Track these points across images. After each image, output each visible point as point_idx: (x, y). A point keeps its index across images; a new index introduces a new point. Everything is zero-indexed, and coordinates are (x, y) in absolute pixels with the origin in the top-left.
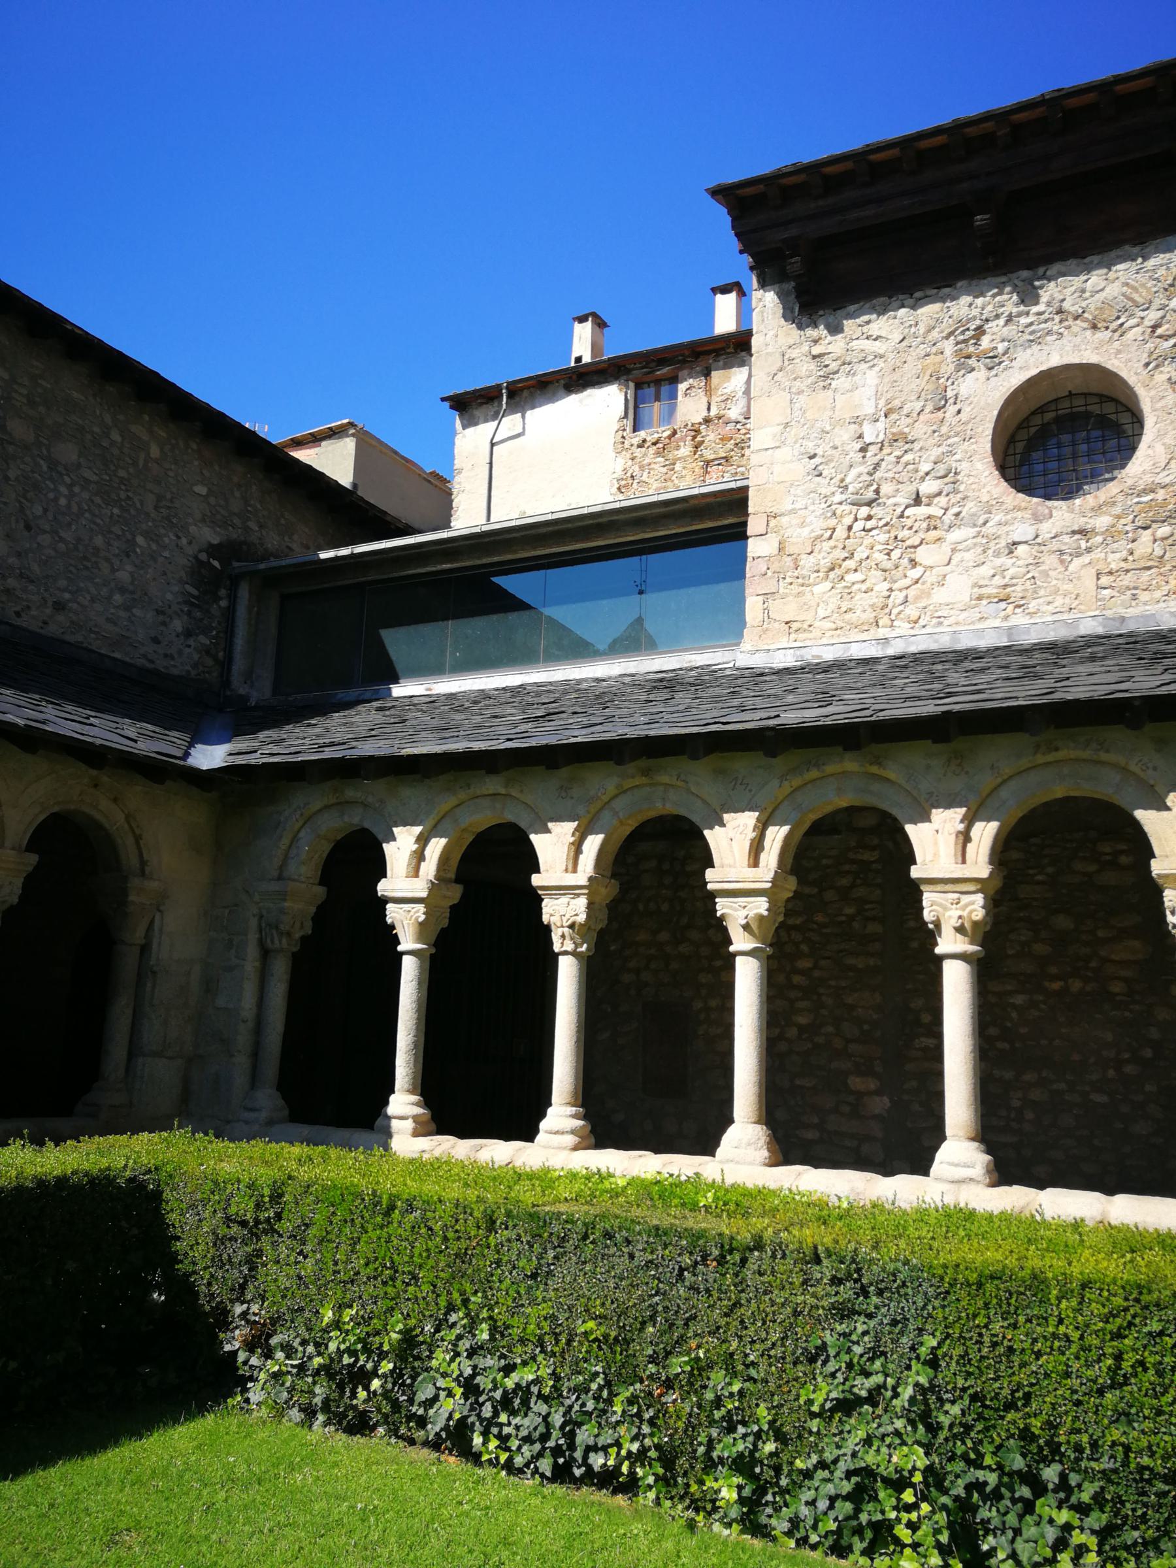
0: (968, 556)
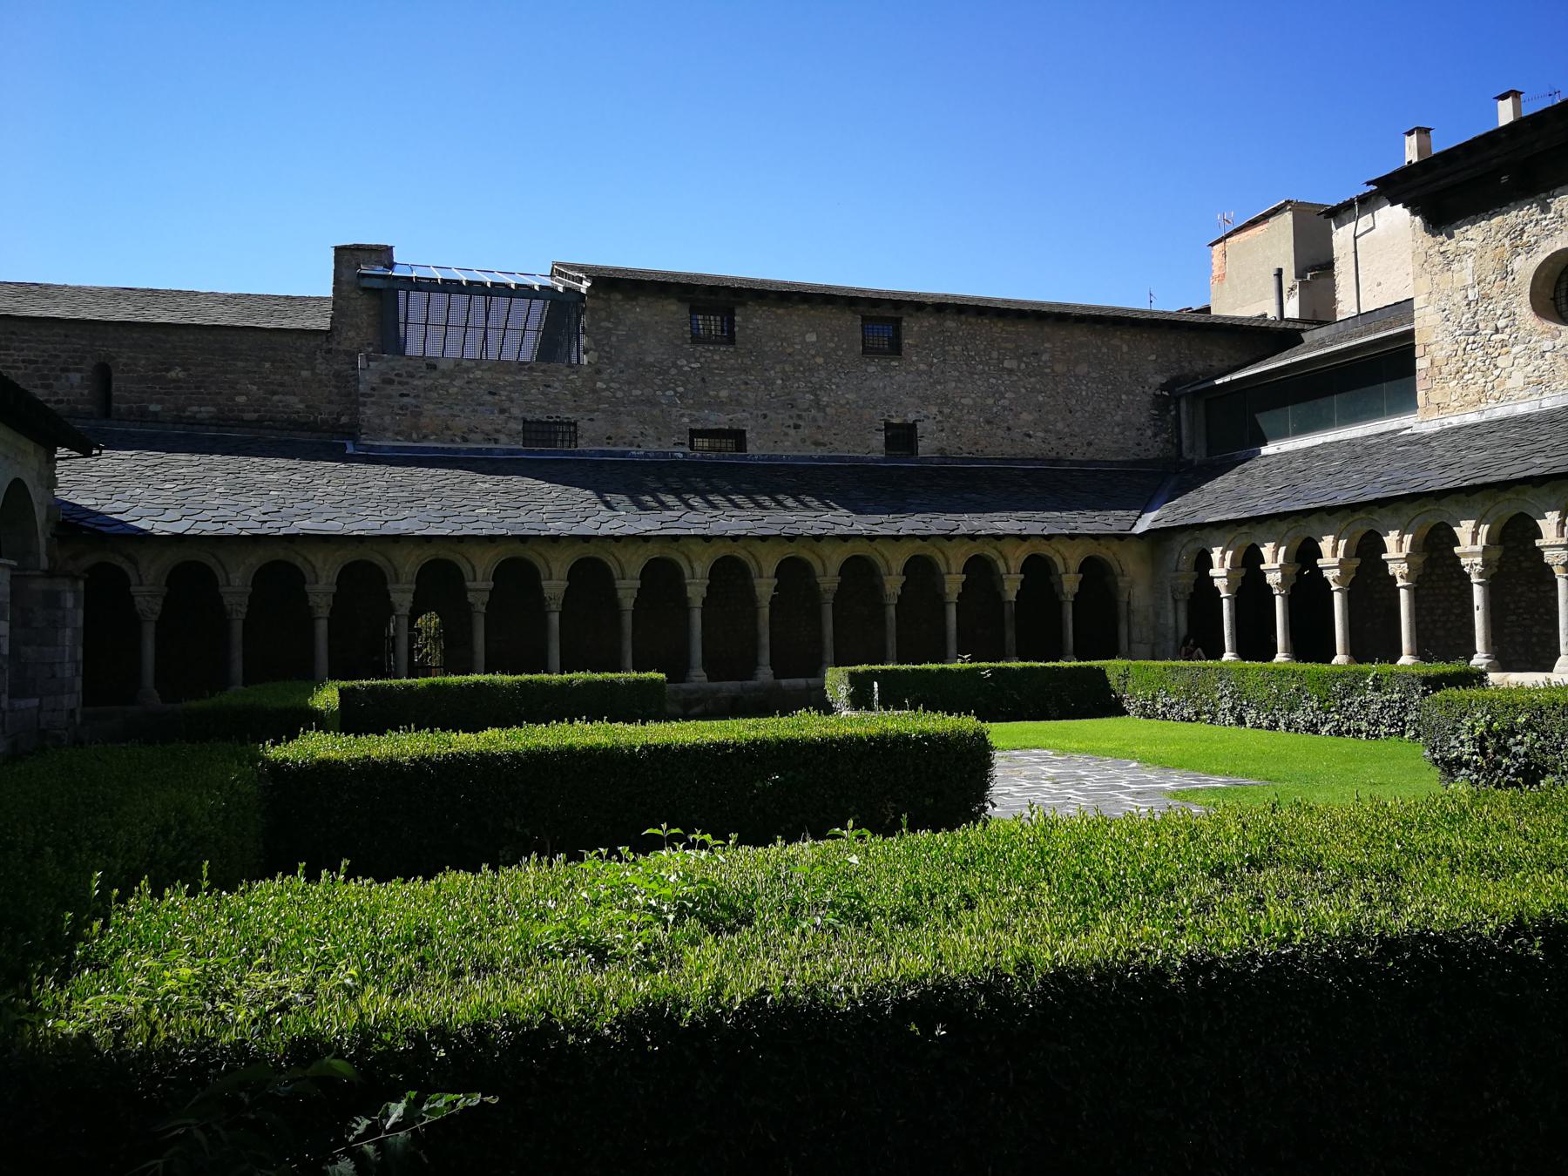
0: (1521, 360)
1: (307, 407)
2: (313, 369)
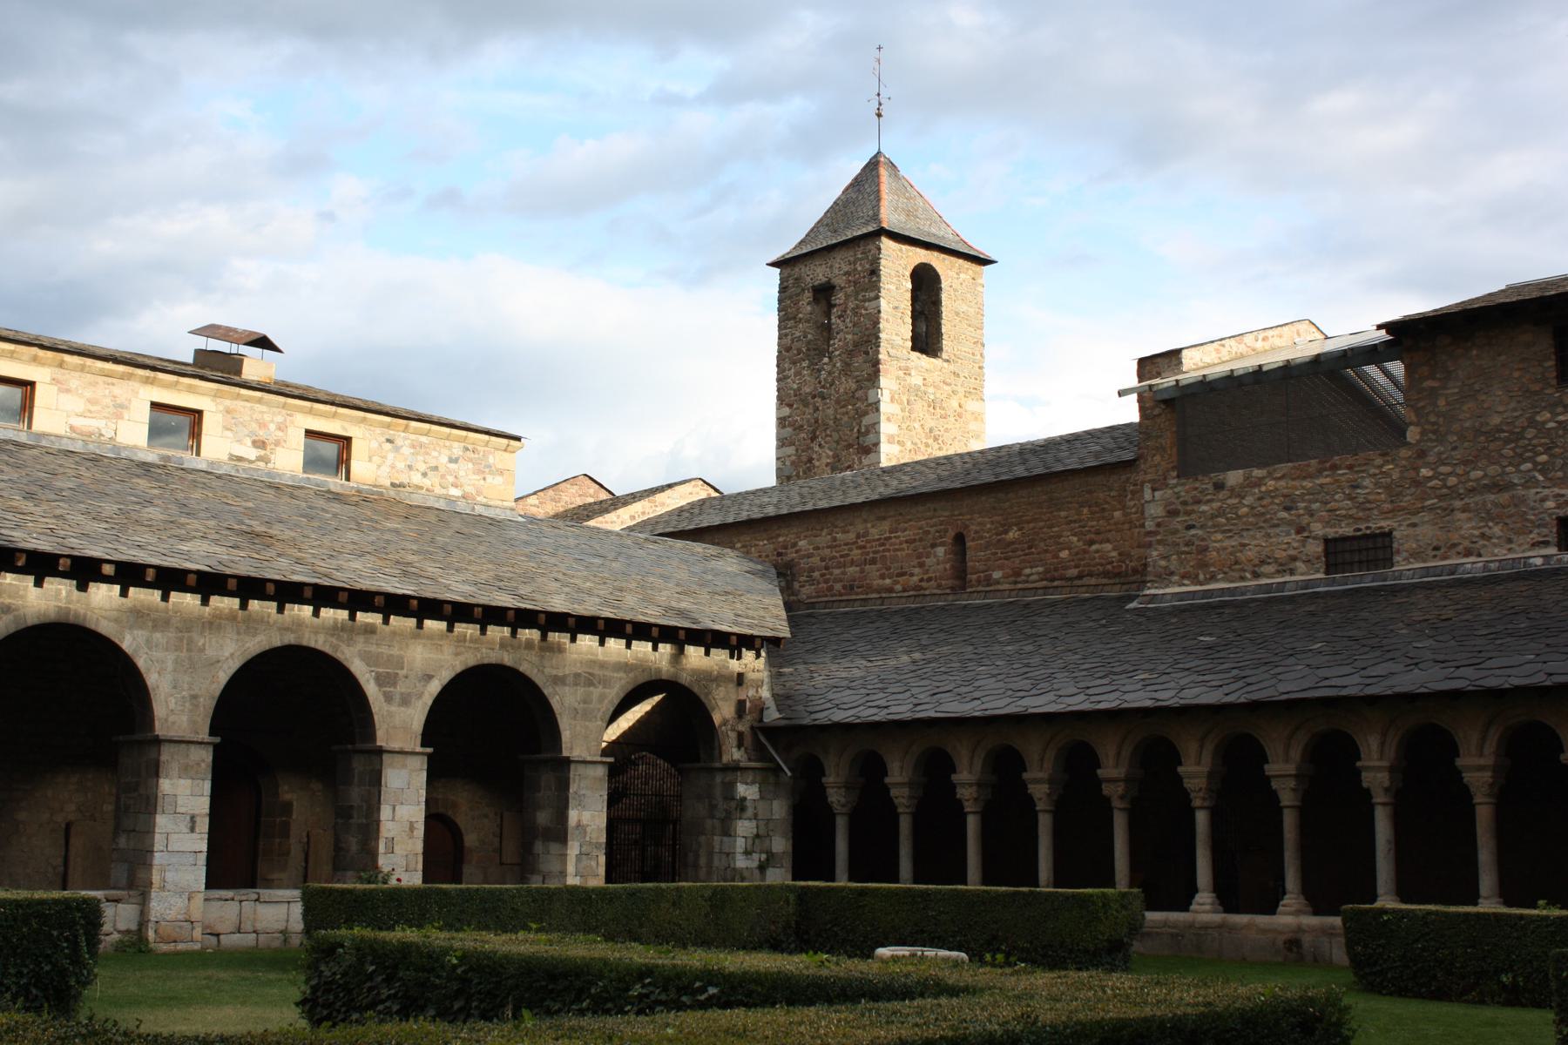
1: (1120, 554)
2: (1124, 508)
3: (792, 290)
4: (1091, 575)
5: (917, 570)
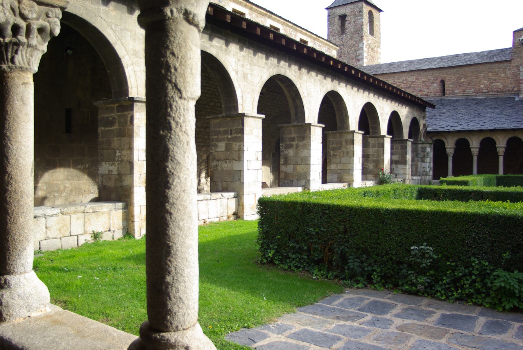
3: (331, 16)
4: (492, 92)
5: (426, 90)
